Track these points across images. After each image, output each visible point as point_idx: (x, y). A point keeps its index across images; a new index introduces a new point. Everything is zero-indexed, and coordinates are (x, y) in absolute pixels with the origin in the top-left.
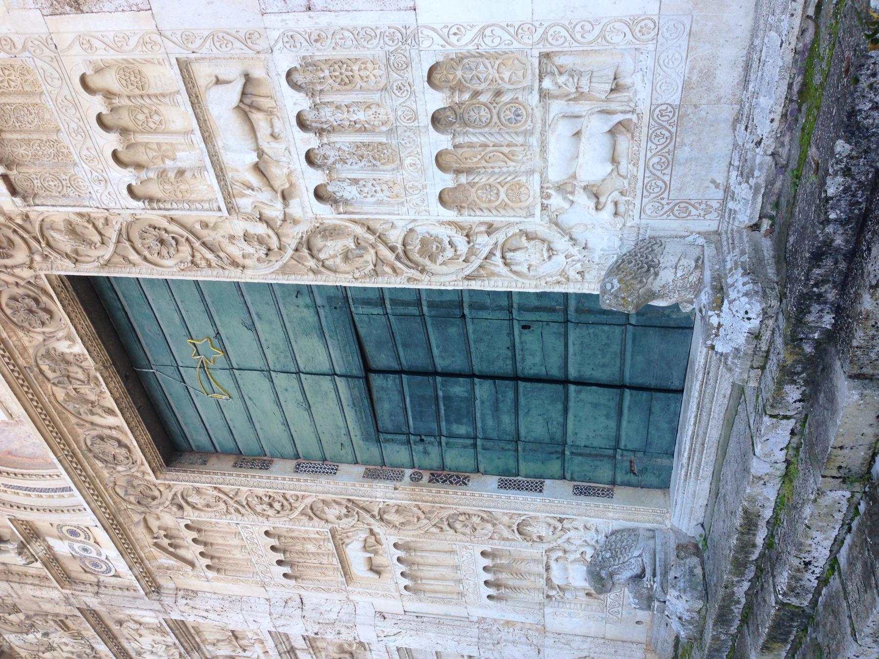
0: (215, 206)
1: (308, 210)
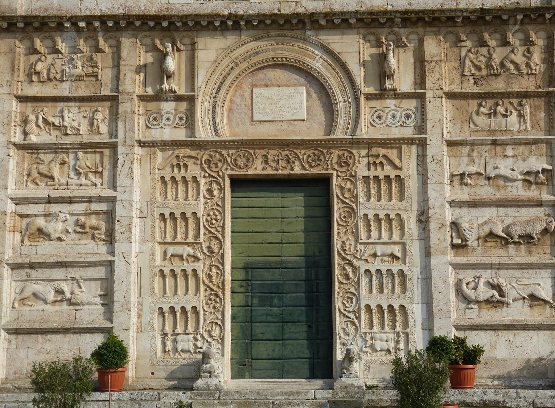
0: (362, 238)
1: (363, 266)
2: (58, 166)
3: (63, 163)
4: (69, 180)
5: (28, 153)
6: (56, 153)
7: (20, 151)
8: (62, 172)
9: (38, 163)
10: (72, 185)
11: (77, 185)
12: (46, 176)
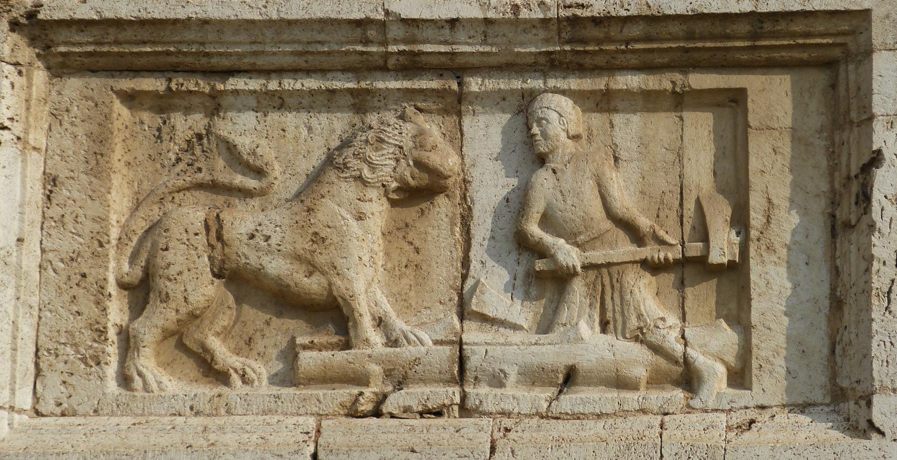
2: (378, 210)
3: (419, 190)
4: (473, 334)
5: (130, 98)
6: (361, 102)
7: (74, 85)
8: (407, 264)
9: (214, 187)
10: (498, 381)
11: (534, 376)
12: (283, 300)
